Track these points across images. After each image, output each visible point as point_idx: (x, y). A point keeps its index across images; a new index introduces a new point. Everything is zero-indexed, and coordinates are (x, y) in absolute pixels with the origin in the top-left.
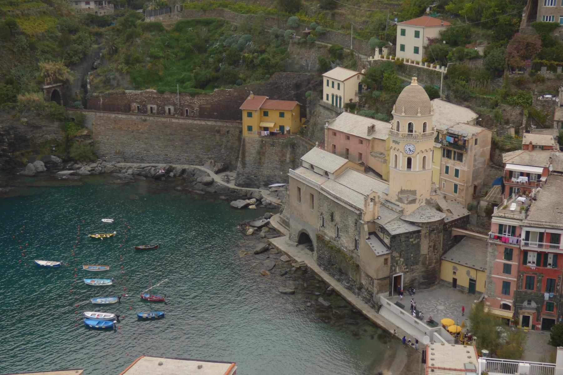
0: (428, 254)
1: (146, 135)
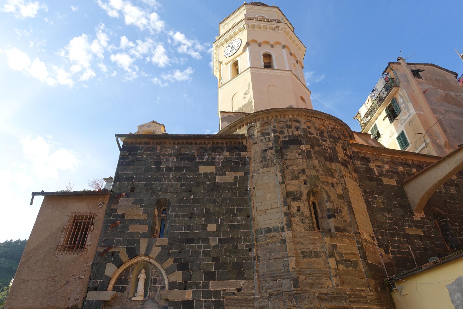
0: (289, 225)
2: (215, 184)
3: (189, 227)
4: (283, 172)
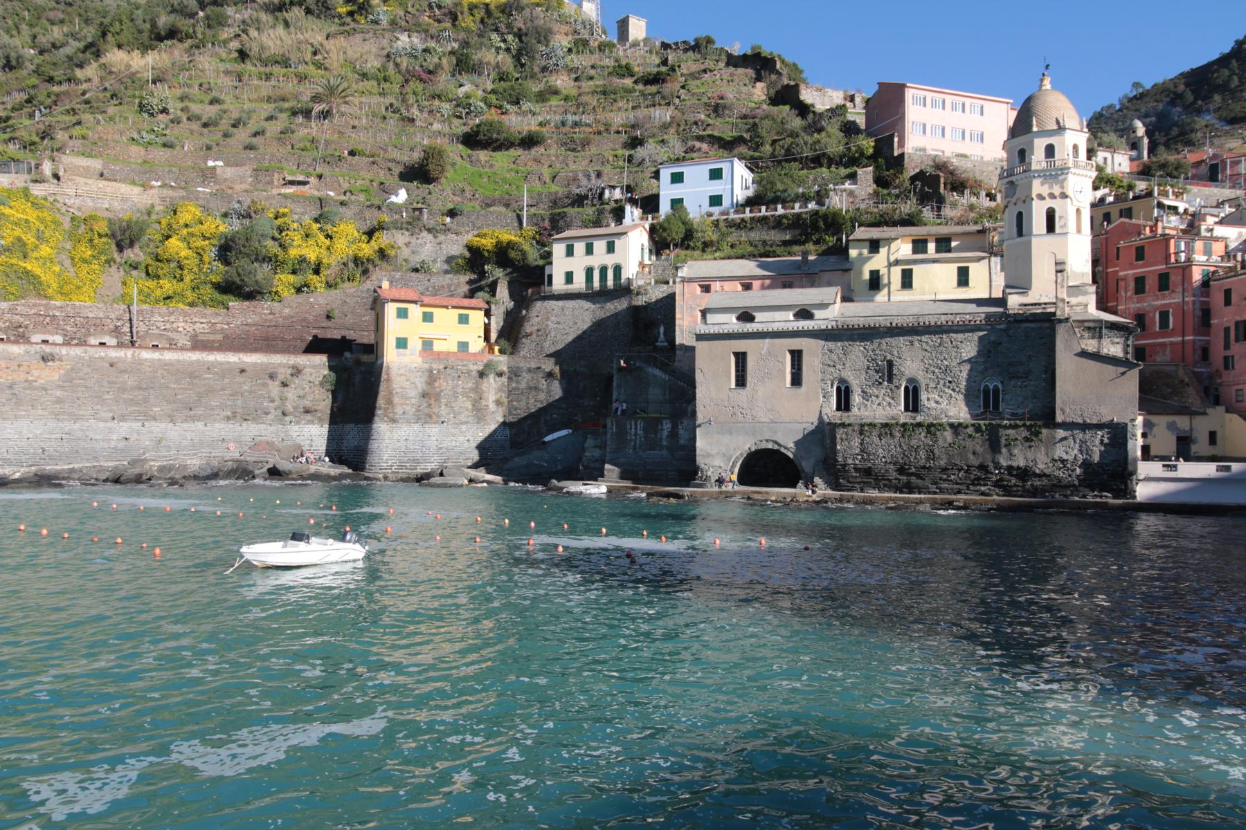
1: (59, 393)
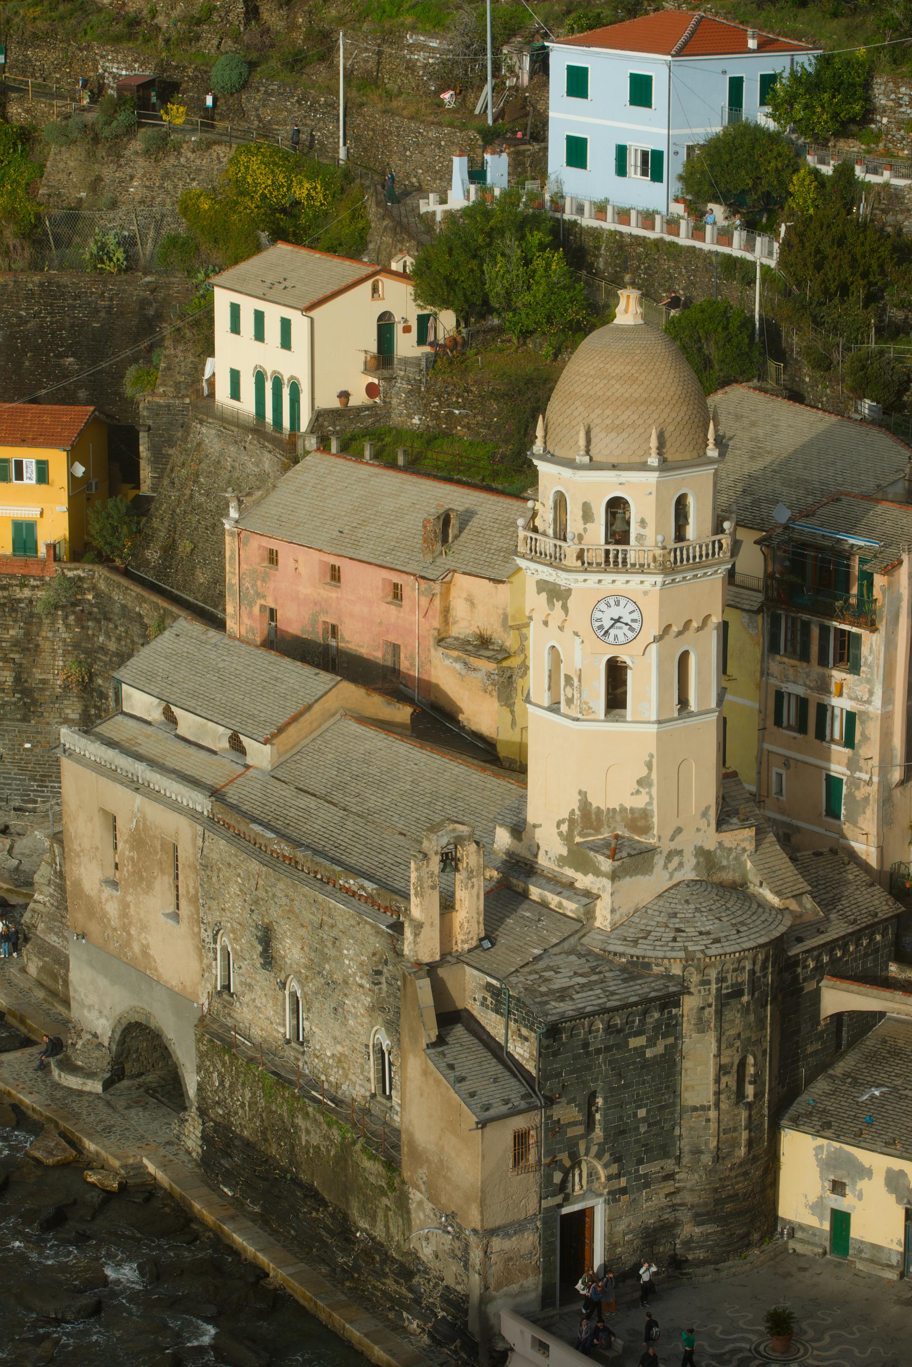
2: (646, 1060)
3: (621, 1118)
4: (719, 1041)
